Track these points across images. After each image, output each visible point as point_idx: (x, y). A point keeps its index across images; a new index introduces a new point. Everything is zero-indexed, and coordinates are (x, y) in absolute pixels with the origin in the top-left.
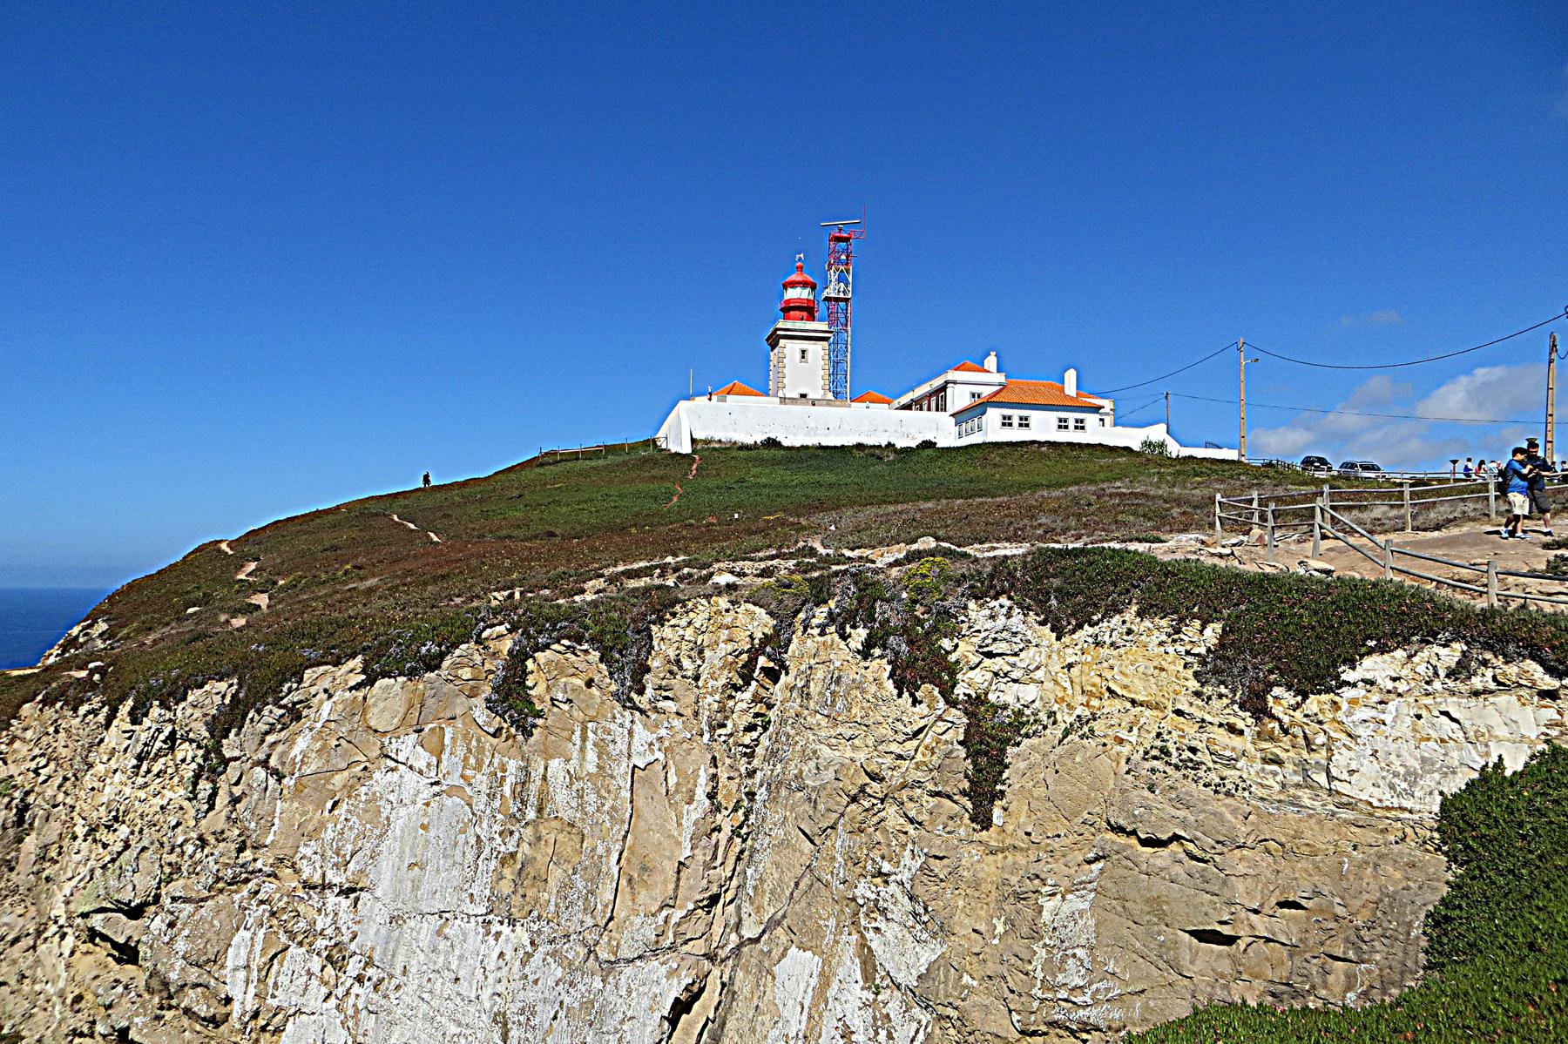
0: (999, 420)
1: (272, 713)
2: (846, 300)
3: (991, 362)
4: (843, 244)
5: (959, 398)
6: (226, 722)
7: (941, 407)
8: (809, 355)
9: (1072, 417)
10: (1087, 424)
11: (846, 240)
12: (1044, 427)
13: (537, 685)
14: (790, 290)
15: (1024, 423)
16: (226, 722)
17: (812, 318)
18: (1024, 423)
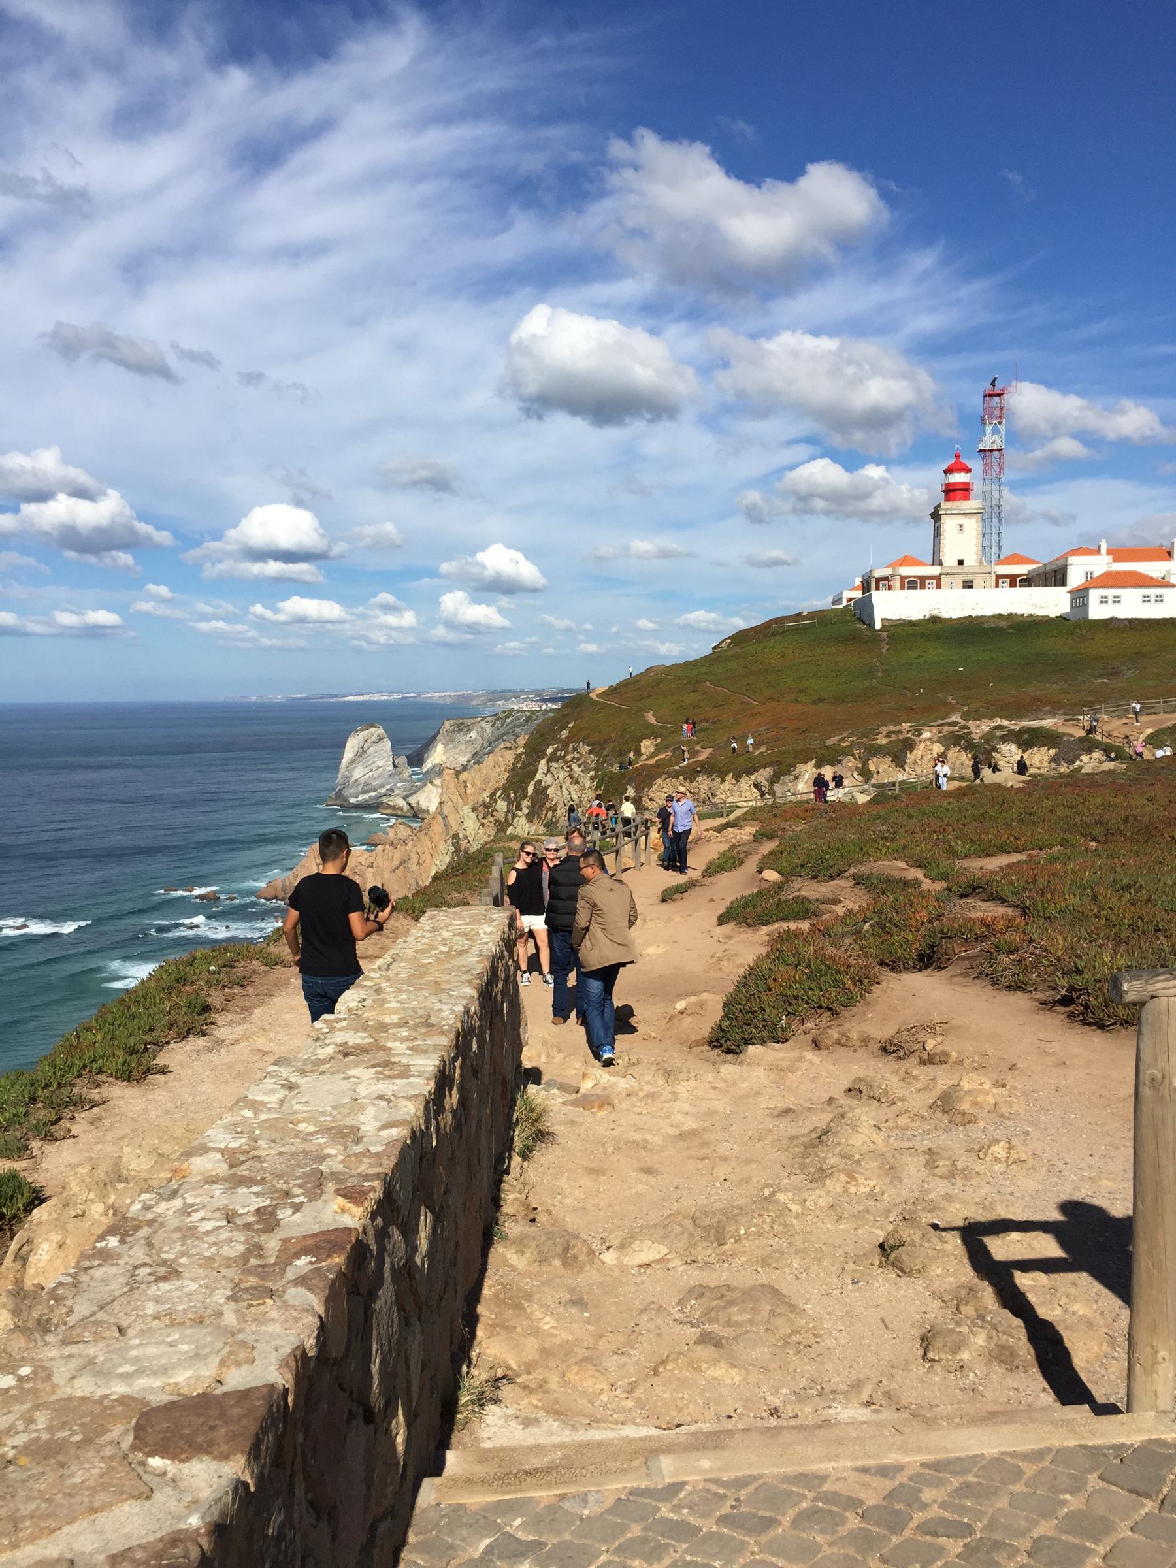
0: (1098, 600)
1: (788, 778)
2: (999, 450)
3: (1104, 547)
4: (997, 399)
5: (1075, 578)
6: (773, 780)
7: (1063, 583)
8: (965, 528)
9: (1153, 592)
10: (1165, 598)
11: (999, 395)
12: (1131, 605)
13: (872, 768)
14: (949, 476)
15: (1117, 600)
16: (773, 780)
17: (967, 498)
18: (1117, 600)
